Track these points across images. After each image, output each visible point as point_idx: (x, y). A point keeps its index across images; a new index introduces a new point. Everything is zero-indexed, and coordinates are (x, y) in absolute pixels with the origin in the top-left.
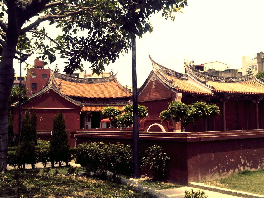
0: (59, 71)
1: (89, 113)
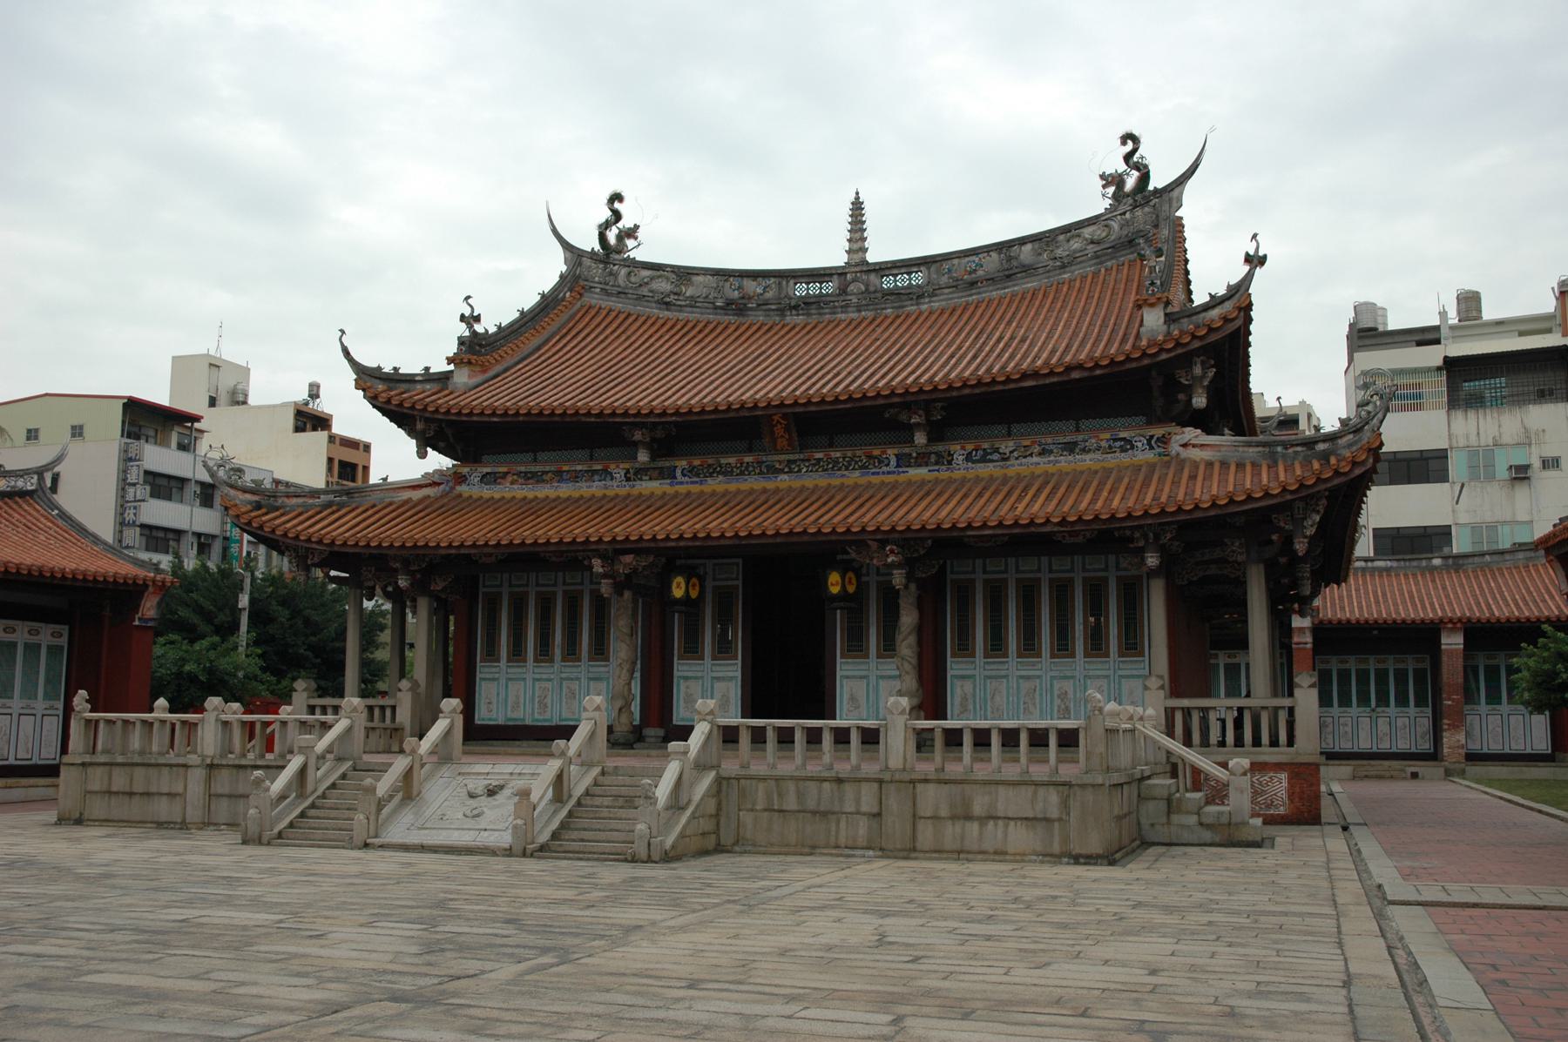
0: (630, 243)
1: (628, 559)
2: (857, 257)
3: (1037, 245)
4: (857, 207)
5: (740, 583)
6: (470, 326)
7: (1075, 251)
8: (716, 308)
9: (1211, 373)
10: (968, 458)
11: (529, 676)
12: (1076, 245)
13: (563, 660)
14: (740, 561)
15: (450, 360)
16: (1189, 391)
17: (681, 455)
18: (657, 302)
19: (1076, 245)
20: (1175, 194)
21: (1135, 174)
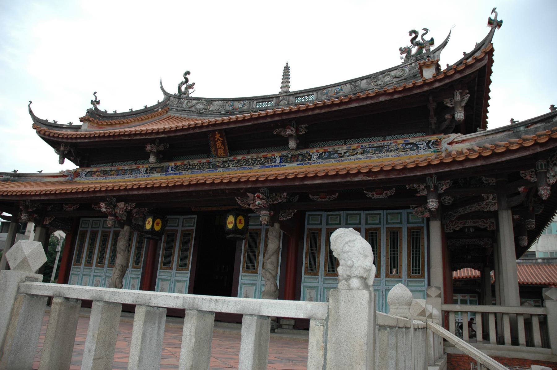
1: (121, 205)
2: (285, 90)
3: (369, 80)
4: (287, 69)
5: (194, 228)
6: (95, 106)
7: (387, 82)
8: (221, 114)
9: (467, 98)
10: (320, 157)
11: (92, 274)
12: (387, 79)
13: (108, 267)
14: (196, 216)
15: (82, 120)
16: (452, 111)
17: (171, 160)
18: (197, 113)
19: (387, 79)
20: (436, 54)
21: (416, 48)
